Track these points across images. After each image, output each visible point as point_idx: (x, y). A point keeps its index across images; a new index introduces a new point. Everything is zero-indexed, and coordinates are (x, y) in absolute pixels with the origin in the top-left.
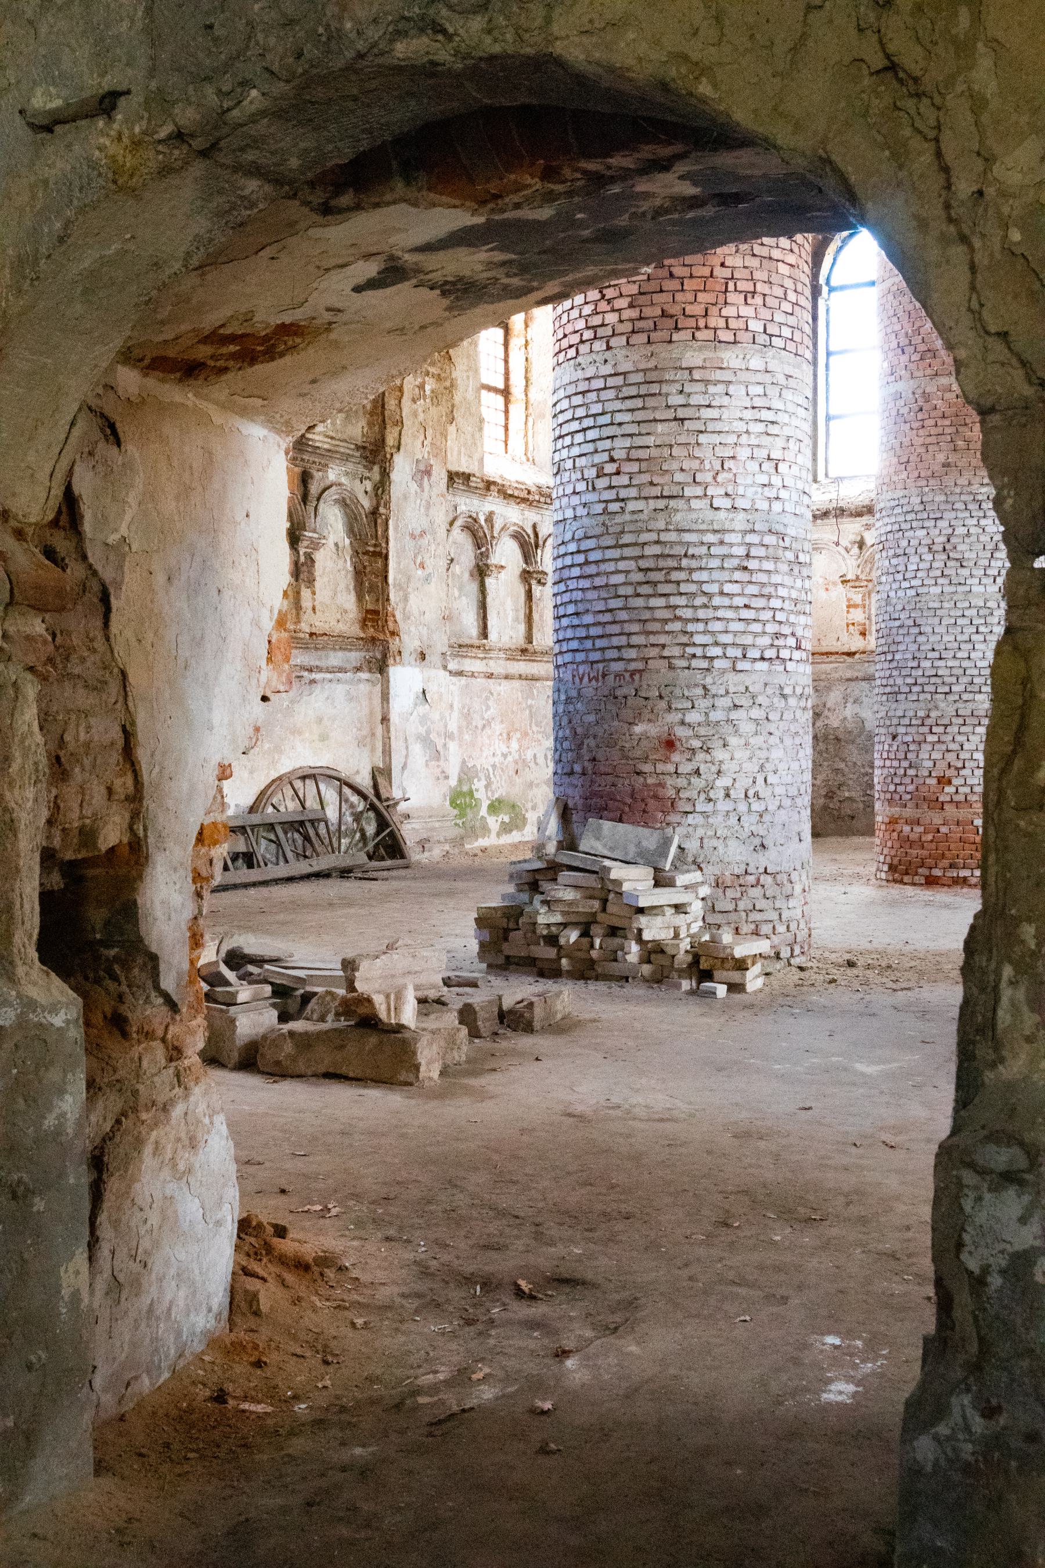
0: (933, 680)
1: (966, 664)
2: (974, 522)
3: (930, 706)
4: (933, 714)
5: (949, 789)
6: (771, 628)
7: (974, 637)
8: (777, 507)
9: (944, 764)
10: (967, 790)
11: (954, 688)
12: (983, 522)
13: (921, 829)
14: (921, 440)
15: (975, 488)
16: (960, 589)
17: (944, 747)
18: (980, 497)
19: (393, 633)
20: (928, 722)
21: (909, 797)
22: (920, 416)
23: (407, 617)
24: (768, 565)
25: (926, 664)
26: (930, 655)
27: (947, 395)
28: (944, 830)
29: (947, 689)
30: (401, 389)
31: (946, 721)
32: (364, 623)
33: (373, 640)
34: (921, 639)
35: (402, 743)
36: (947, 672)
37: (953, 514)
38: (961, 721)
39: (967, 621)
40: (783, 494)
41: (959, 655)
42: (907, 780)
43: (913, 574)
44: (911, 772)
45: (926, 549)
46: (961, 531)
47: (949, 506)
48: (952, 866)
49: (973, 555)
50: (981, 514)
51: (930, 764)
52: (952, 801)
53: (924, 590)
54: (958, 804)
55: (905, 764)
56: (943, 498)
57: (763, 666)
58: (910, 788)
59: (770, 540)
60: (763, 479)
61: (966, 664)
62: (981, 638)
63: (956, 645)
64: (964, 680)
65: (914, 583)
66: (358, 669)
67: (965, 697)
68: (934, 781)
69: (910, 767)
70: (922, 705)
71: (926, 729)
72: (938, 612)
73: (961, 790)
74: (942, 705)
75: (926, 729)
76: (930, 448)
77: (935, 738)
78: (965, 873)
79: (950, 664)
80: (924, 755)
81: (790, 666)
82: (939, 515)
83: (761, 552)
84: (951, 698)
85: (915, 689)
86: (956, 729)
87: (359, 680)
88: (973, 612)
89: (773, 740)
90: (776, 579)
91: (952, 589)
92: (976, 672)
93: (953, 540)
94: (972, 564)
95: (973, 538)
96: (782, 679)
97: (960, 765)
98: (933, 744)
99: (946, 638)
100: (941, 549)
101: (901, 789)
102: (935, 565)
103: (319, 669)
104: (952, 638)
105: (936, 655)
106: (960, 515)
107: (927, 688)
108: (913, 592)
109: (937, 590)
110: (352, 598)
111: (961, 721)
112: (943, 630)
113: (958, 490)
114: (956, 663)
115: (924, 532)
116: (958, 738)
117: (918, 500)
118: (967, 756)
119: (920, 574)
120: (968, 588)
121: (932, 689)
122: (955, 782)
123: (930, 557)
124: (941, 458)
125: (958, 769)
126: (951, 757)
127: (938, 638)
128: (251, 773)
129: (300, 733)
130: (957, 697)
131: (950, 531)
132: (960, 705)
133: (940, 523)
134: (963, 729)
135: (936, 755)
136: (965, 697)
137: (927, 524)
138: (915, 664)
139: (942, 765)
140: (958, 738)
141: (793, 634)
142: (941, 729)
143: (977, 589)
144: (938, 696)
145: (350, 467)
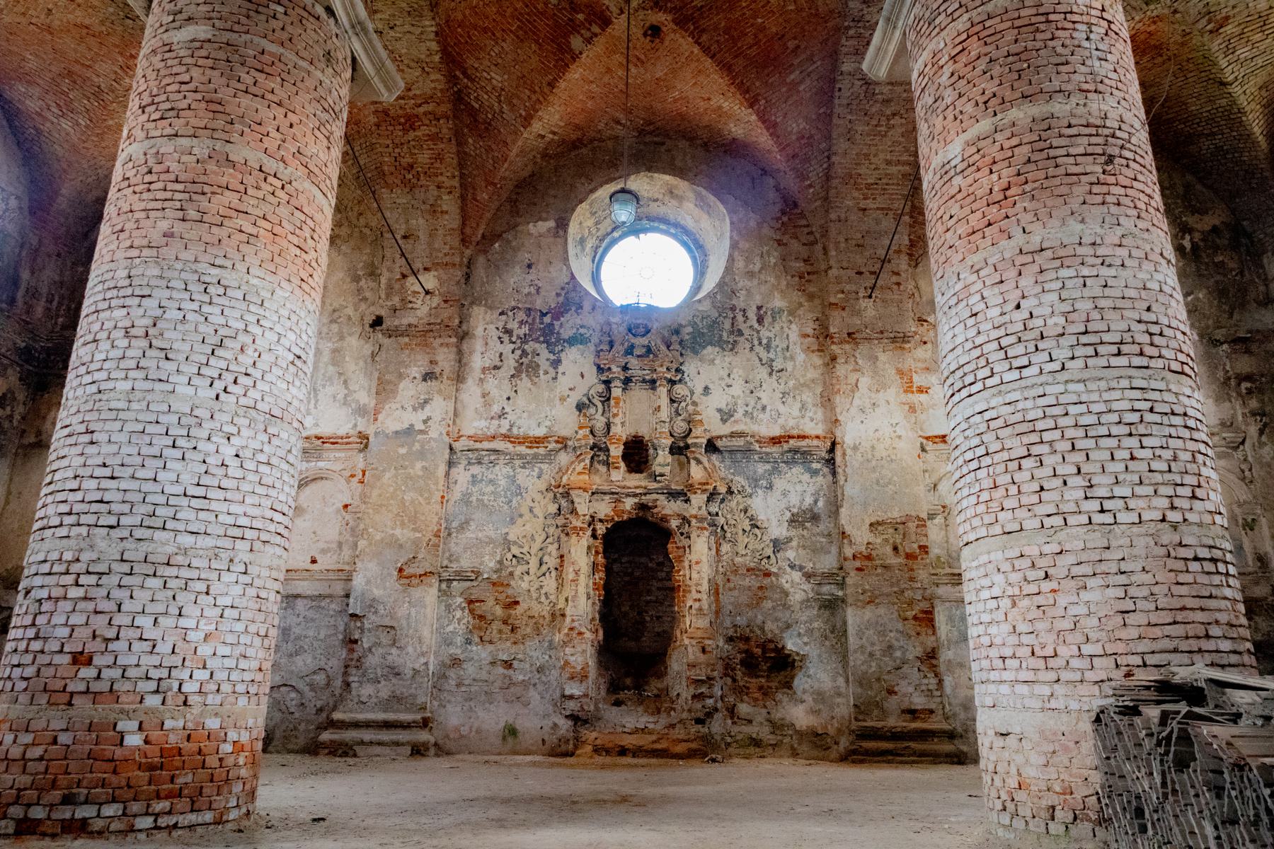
0: (95, 507)
1: (148, 487)
2: (195, 306)
3: (83, 545)
4: (85, 557)
5: (87, 672)
7: (169, 452)
9: (86, 632)
10: (116, 673)
11: (124, 521)
12: (206, 309)
13: (28, 738)
14: (143, 205)
15: (202, 267)
16: (159, 386)
17: (90, 606)
18: (207, 279)
20: (75, 568)
21: (23, 684)
22: (148, 178)
25: (92, 484)
26: (100, 472)
27: (185, 158)
28: (64, 738)
29: (112, 521)
31: (102, 568)
34: (91, 450)
36: (118, 496)
37: (167, 293)
38: (125, 568)
39: (161, 429)
41: (140, 474)
42: (28, 658)
43: (98, 366)
44: (36, 646)
45: (122, 332)
46: (173, 314)
47: (164, 283)
48: (68, 800)
49: (186, 347)
50: (206, 298)
51: (66, 631)
52: (87, 692)
53: (110, 385)
54: (95, 696)
55: (31, 633)
56: (156, 272)
58: (29, 672)
61: (148, 487)
62: (178, 454)
63: (138, 460)
64: (143, 509)
65: (97, 376)
67: (139, 533)
68: (66, 659)
69: (37, 637)
70: (72, 542)
71: (69, 579)
72: (122, 415)
73: (106, 674)
74: (102, 545)
75: (69, 579)
76: (152, 214)
77: (79, 593)
78: (83, 812)
79: (123, 485)
80: (59, 619)
82: (146, 292)
84: (116, 533)
85: (68, 520)
86: (114, 579)
88: (174, 419)
91: (148, 385)
92: (162, 500)
93: (160, 325)
94: (182, 357)
95: (188, 327)
97: (111, 634)
98: (76, 601)
99: (125, 450)
100: (141, 332)
101: (17, 672)
102: (129, 353)
104: (134, 451)
105: (107, 472)
106: (175, 295)
107: (84, 519)
108: (94, 388)
109: (127, 385)
111: (125, 568)
112: (123, 438)
113: (179, 266)
114: (134, 485)
115: (124, 311)
116: (121, 594)
117: (124, 273)
118: (126, 620)
119: (107, 365)
120: (170, 388)
121: (91, 519)
122: (97, 660)
123: (125, 343)
124: (164, 225)
125: (107, 640)
126: (99, 622)
127: (114, 448)
130: (126, 533)
131: (159, 312)
132: (129, 544)
133: (145, 302)
134: (127, 581)
135: (77, 619)
136: (139, 533)
137: (128, 302)
138: (74, 484)
139: (84, 633)
140: (116, 594)
142: (92, 580)
143: (183, 390)
144: (98, 530)
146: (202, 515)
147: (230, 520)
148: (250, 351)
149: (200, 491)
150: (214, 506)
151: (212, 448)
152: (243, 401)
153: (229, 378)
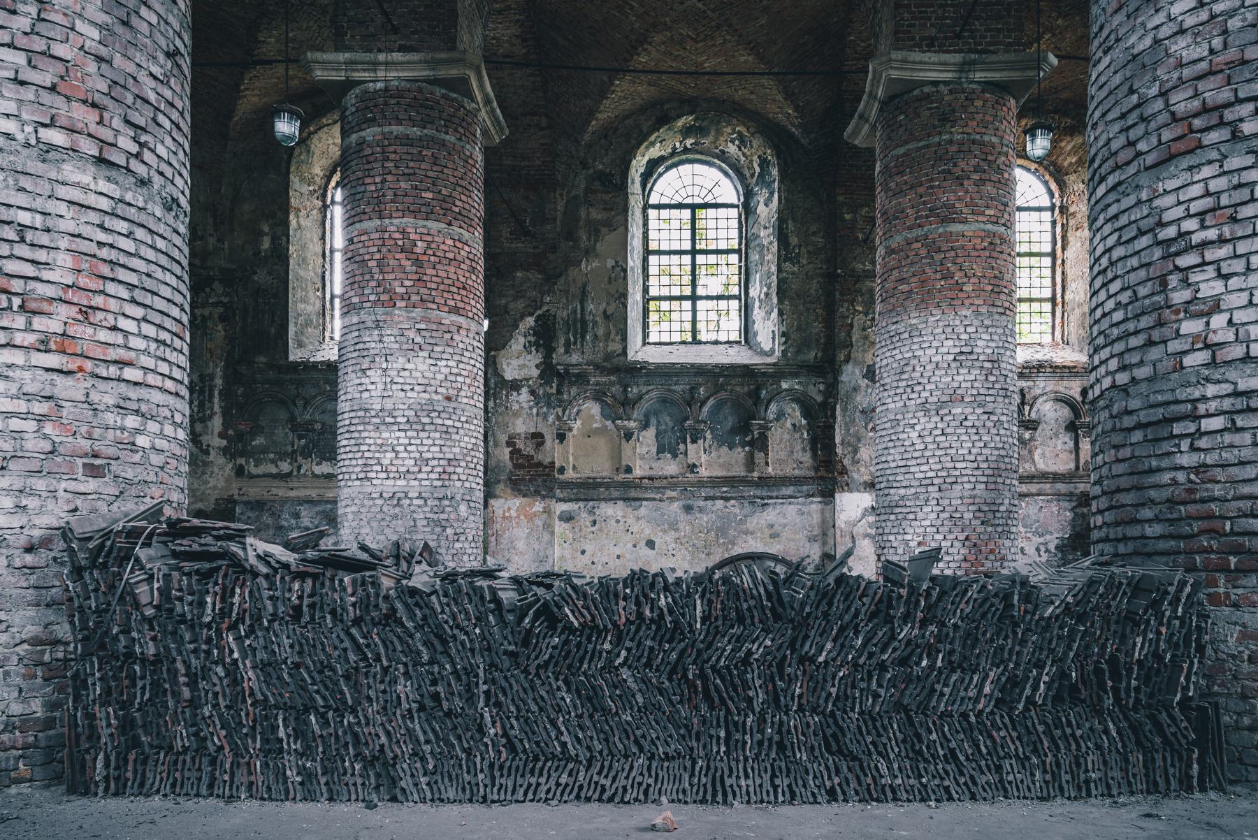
6: (360, 462)
8: (366, 395)
19: (841, 473)
23: (856, 462)
24: (360, 428)
30: (851, 325)
32: (816, 469)
33: (821, 478)
35: (848, 539)
40: (370, 387)
57: (358, 483)
59: (361, 413)
60: (358, 381)
66: (812, 496)
81: (374, 482)
83: (355, 421)
87: (812, 503)
89: (362, 523)
90: (365, 434)
96: (369, 490)
103: (771, 498)
110: (808, 455)
128: (708, 555)
129: (752, 533)
141: (379, 464)
145: (803, 379)
146: (907, 476)
147: (922, 475)
148: (918, 369)
149: (903, 463)
150: (912, 469)
151: (905, 436)
152: (919, 401)
153: (909, 390)
